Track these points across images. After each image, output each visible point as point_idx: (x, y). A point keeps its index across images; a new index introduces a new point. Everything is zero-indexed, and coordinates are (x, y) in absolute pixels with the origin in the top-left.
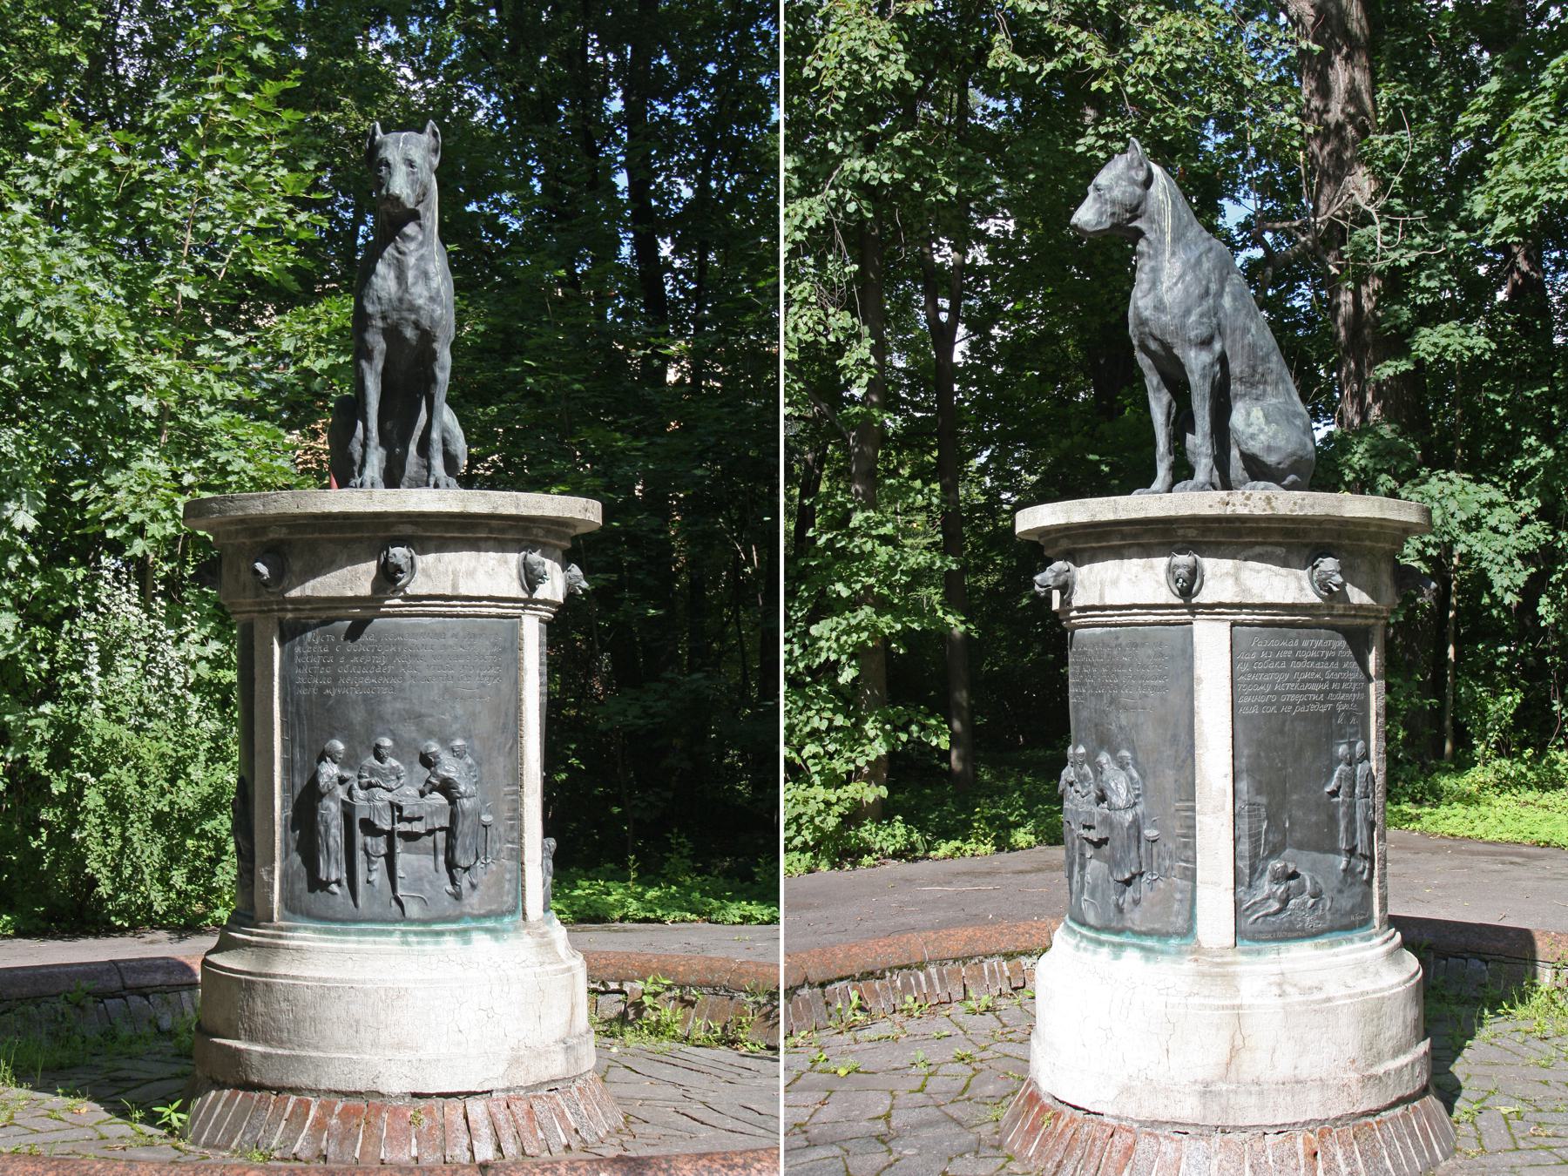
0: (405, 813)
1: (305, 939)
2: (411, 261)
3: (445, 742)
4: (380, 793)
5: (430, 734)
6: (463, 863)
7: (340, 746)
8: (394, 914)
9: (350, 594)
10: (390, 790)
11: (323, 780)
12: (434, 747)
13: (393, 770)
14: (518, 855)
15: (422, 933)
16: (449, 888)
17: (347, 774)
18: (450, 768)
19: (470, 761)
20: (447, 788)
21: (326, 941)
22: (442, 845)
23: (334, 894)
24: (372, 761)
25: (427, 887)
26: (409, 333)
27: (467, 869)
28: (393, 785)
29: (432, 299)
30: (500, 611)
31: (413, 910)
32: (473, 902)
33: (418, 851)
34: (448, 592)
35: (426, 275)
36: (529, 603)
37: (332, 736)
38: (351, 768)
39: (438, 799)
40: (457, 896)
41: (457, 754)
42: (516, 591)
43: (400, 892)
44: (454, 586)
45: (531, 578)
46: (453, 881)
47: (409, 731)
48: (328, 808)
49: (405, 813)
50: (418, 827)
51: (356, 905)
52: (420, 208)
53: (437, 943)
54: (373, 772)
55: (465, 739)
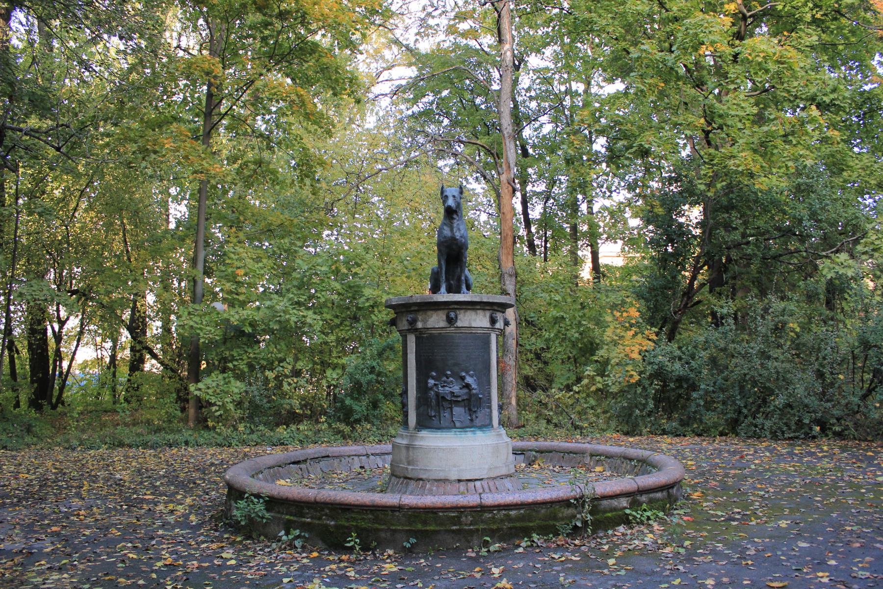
2: (455, 225)
3: (467, 372)
4: (447, 388)
5: (463, 371)
7: (434, 374)
8: (452, 426)
11: (429, 385)
12: (464, 374)
14: (490, 407)
18: (469, 380)
20: (468, 386)
24: (445, 378)
26: (454, 247)
31: (458, 424)
32: (477, 422)
33: (459, 406)
35: (459, 229)
36: (493, 329)
39: (465, 391)
40: (472, 420)
41: (472, 376)
42: (488, 325)
44: (470, 323)
45: (493, 321)
46: (470, 415)
47: (456, 369)
50: (459, 399)
54: (445, 382)
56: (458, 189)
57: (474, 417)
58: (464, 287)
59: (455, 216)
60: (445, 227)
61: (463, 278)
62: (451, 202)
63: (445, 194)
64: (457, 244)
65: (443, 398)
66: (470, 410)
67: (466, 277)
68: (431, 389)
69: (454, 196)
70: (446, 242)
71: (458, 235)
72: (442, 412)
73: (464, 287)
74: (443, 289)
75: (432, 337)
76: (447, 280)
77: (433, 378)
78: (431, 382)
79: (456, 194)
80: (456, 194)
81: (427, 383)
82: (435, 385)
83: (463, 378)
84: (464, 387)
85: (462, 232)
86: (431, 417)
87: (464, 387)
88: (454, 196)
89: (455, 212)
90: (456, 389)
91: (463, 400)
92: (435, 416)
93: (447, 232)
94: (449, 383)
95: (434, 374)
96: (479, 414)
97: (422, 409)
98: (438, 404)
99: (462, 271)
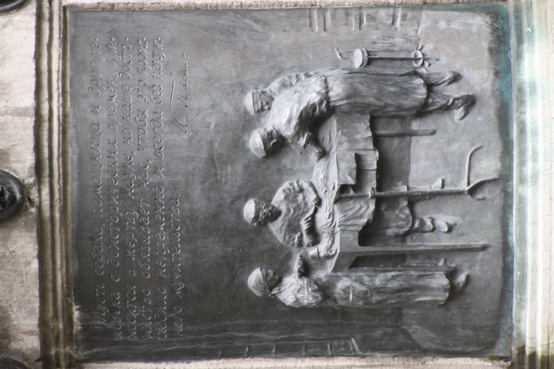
0: (351, 181)
1: (533, 323)
3: (248, 123)
5: (238, 144)
6: (422, 92)
7: (255, 277)
9: (35, 265)
10: (319, 202)
11: (308, 297)
12: (255, 141)
13: (290, 197)
15: (522, 153)
16: (458, 113)
17: (296, 265)
18: (283, 116)
19: (275, 85)
20: (312, 122)
21: (534, 291)
22: (396, 127)
23: (468, 278)
25: (455, 147)
27: (430, 87)
28: (311, 198)
30: (56, 42)
31: (488, 167)
34: (30, 121)
37: (244, 284)
38: (289, 257)
39: (332, 132)
40: (470, 102)
43: (464, 187)
46: (447, 108)
48: (346, 291)
49: (351, 181)
50: (372, 160)
51: (484, 248)
53: (535, 133)
54: (292, 227)
55: (243, 92)
57: (454, 92)
65: (367, 235)
66: (422, 111)
68: (325, 290)
72: (431, 242)
75: (82, 288)
77: (274, 281)
78: (293, 290)
81: (299, 311)
82: (306, 271)
83: (276, 145)
84: (315, 140)
86: (455, 292)
87: (315, 140)
90: (322, 175)
91: (377, 141)
92: (451, 274)
94: (300, 210)
95: (255, 277)
96: (441, 68)
97: (420, 333)
98: (398, 260)
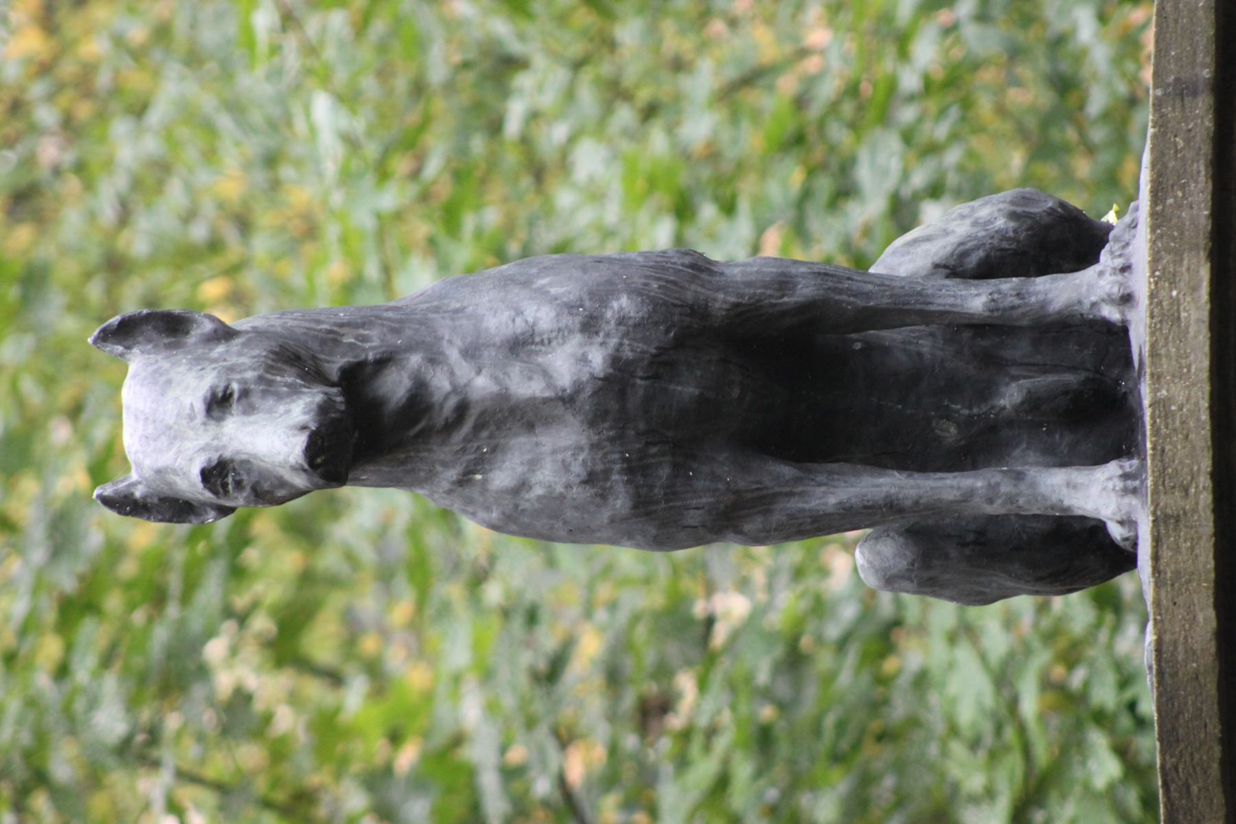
2: (482, 384)
26: (686, 390)
29: (590, 326)
35: (521, 345)
52: (335, 364)
56: (139, 363)
58: (1060, 291)
59: (395, 386)
60: (501, 478)
61: (976, 299)
62: (274, 436)
63: (190, 484)
64: (662, 366)
67: (956, 268)
69: (218, 404)
70: (636, 469)
71: (572, 362)
73: (1060, 291)
74: (1094, 492)
76: (981, 446)
79: (193, 384)
80: (193, 384)
85: (542, 316)
88: (218, 404)
89: (356, 380)
93: (549, 461)
99: (901, 308)
